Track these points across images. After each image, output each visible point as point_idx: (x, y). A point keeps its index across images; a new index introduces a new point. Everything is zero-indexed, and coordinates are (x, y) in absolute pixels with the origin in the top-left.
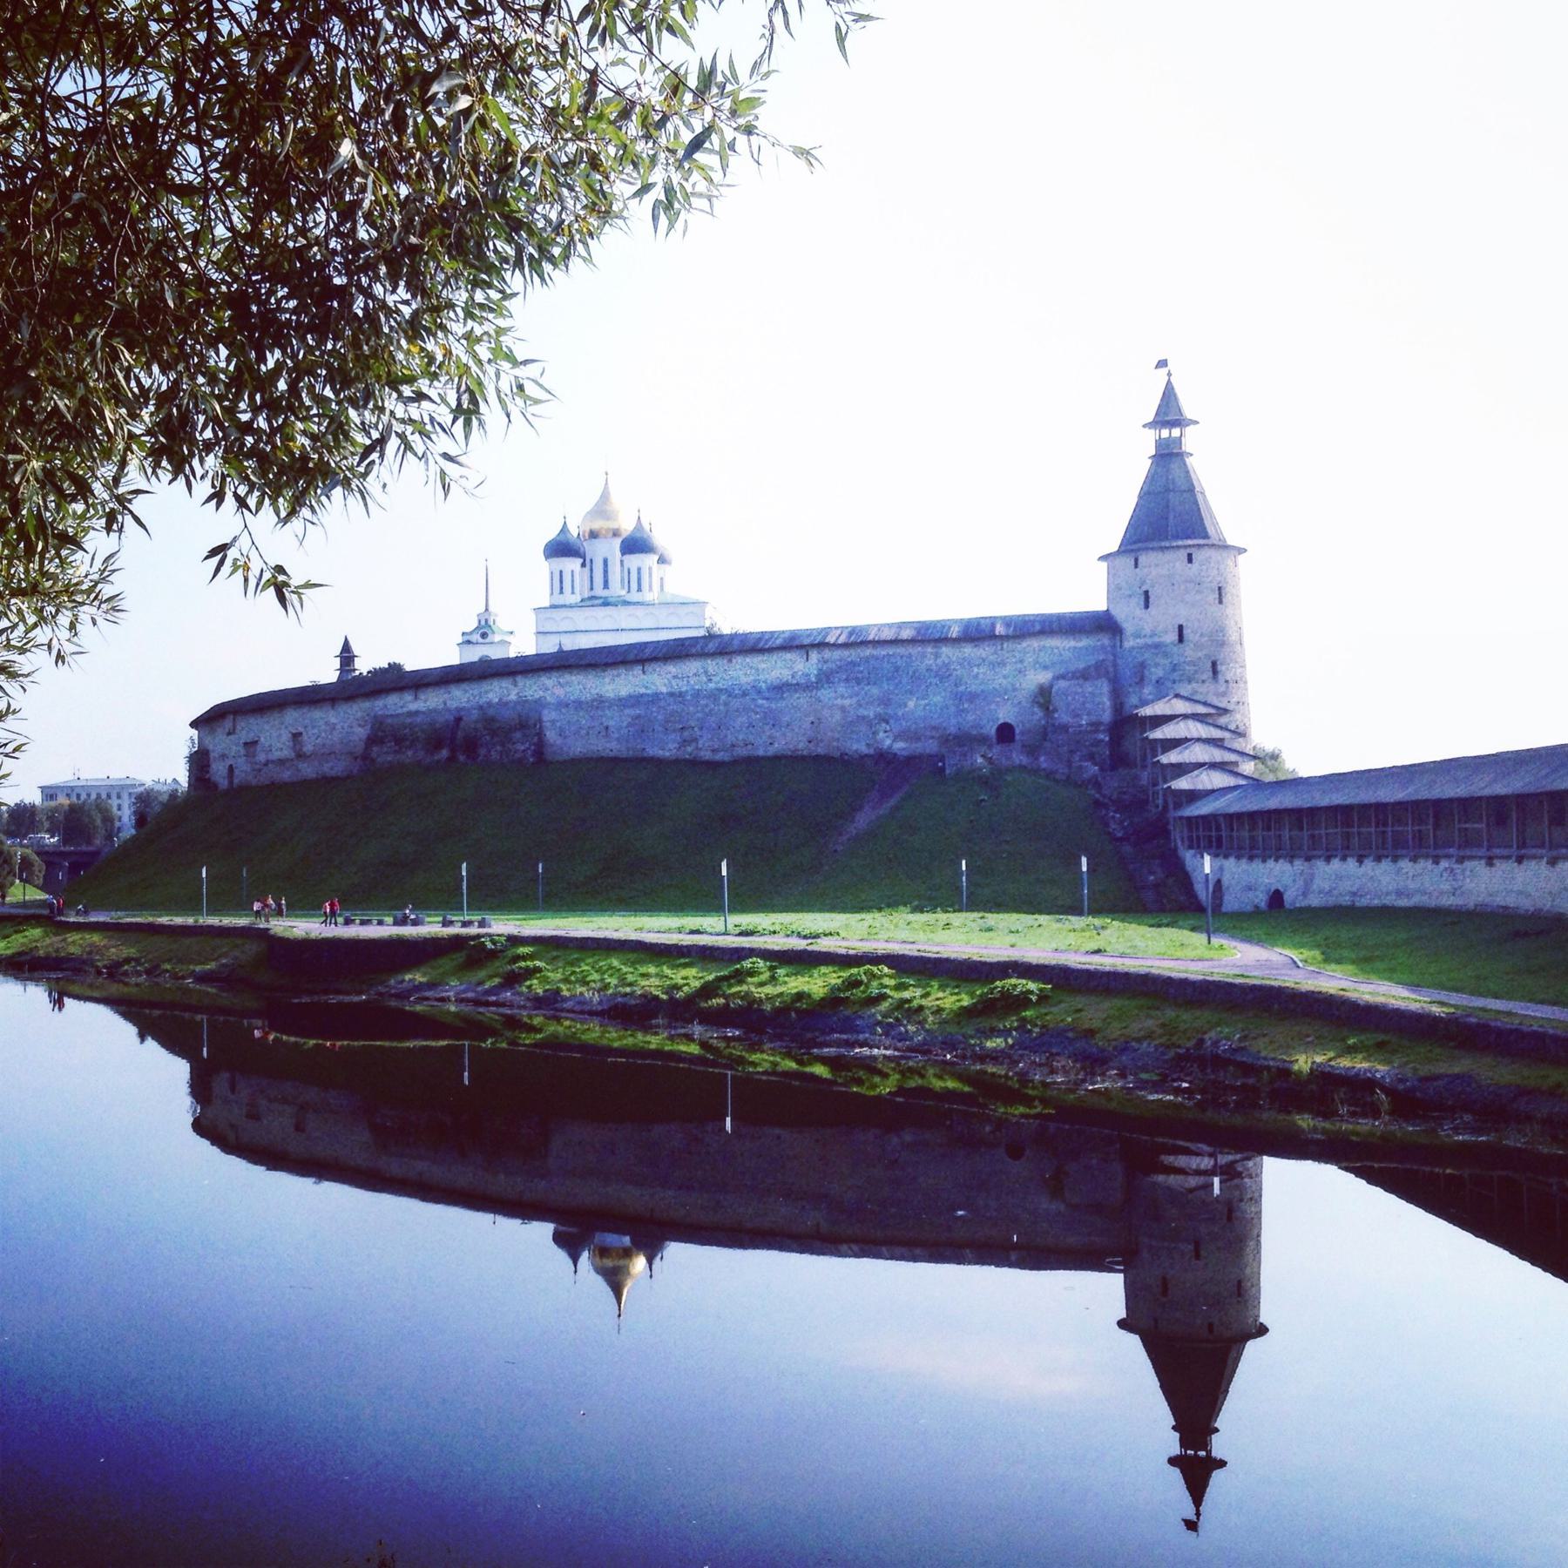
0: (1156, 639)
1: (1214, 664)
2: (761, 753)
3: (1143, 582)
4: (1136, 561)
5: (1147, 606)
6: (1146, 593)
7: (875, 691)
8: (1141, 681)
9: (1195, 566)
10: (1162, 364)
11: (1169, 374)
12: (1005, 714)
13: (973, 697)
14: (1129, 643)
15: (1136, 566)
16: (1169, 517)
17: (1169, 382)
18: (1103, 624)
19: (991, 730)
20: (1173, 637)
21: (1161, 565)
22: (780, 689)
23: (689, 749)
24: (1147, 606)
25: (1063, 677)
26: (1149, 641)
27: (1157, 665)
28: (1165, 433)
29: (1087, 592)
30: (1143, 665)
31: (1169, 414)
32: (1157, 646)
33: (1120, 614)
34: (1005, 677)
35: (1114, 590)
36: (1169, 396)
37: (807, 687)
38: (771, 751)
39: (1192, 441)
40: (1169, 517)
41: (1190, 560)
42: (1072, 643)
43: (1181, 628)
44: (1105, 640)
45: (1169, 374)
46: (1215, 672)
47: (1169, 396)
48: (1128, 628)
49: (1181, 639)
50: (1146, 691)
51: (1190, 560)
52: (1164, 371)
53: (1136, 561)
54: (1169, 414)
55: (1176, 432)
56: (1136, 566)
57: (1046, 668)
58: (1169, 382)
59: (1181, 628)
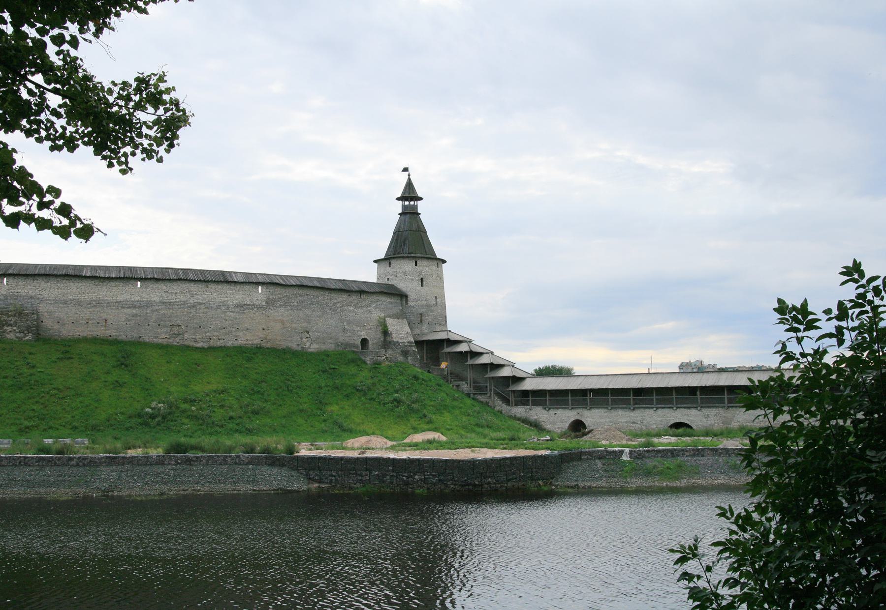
2: (229, 344)
3: (421, 274)
6: (422, 279)
7: (301, 313)
10: (406, 170)
12: (364, 335)
13: (349, 323)
17: (409, 180)
20: (433, 302)
22: (242, 307)
23: (177, 339)
25: (390, 317)
28: (407, 203)
31: (409, 195)
33: (403, 286)
36: (409, 185)
37: (260, 307)
38: (236, 344)
47: (409, 185)
48: (412, 295)
50: (424, 328)
54: (409, 195)
55: (412, 203)
58: (409, 180)
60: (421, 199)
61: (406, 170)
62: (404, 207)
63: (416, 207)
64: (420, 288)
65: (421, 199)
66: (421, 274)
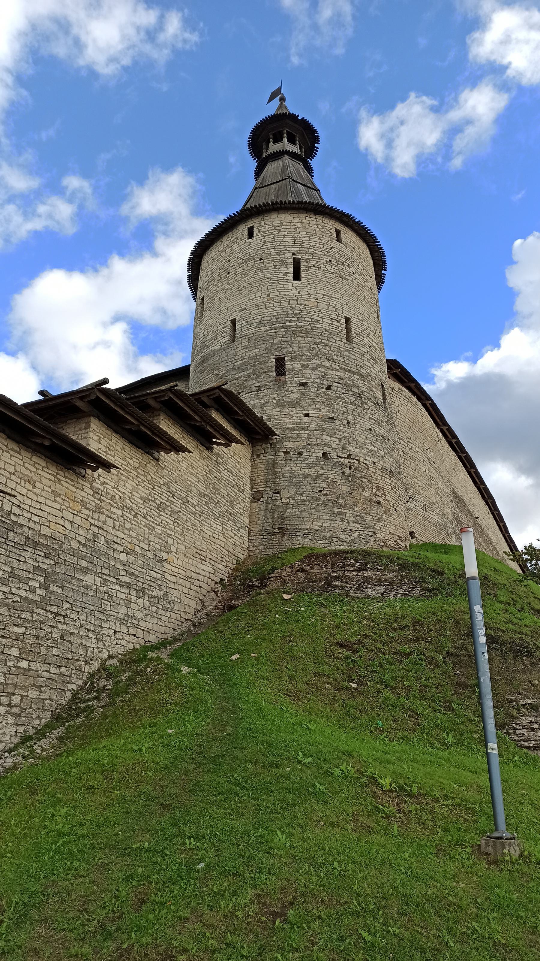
51: (251, 235)
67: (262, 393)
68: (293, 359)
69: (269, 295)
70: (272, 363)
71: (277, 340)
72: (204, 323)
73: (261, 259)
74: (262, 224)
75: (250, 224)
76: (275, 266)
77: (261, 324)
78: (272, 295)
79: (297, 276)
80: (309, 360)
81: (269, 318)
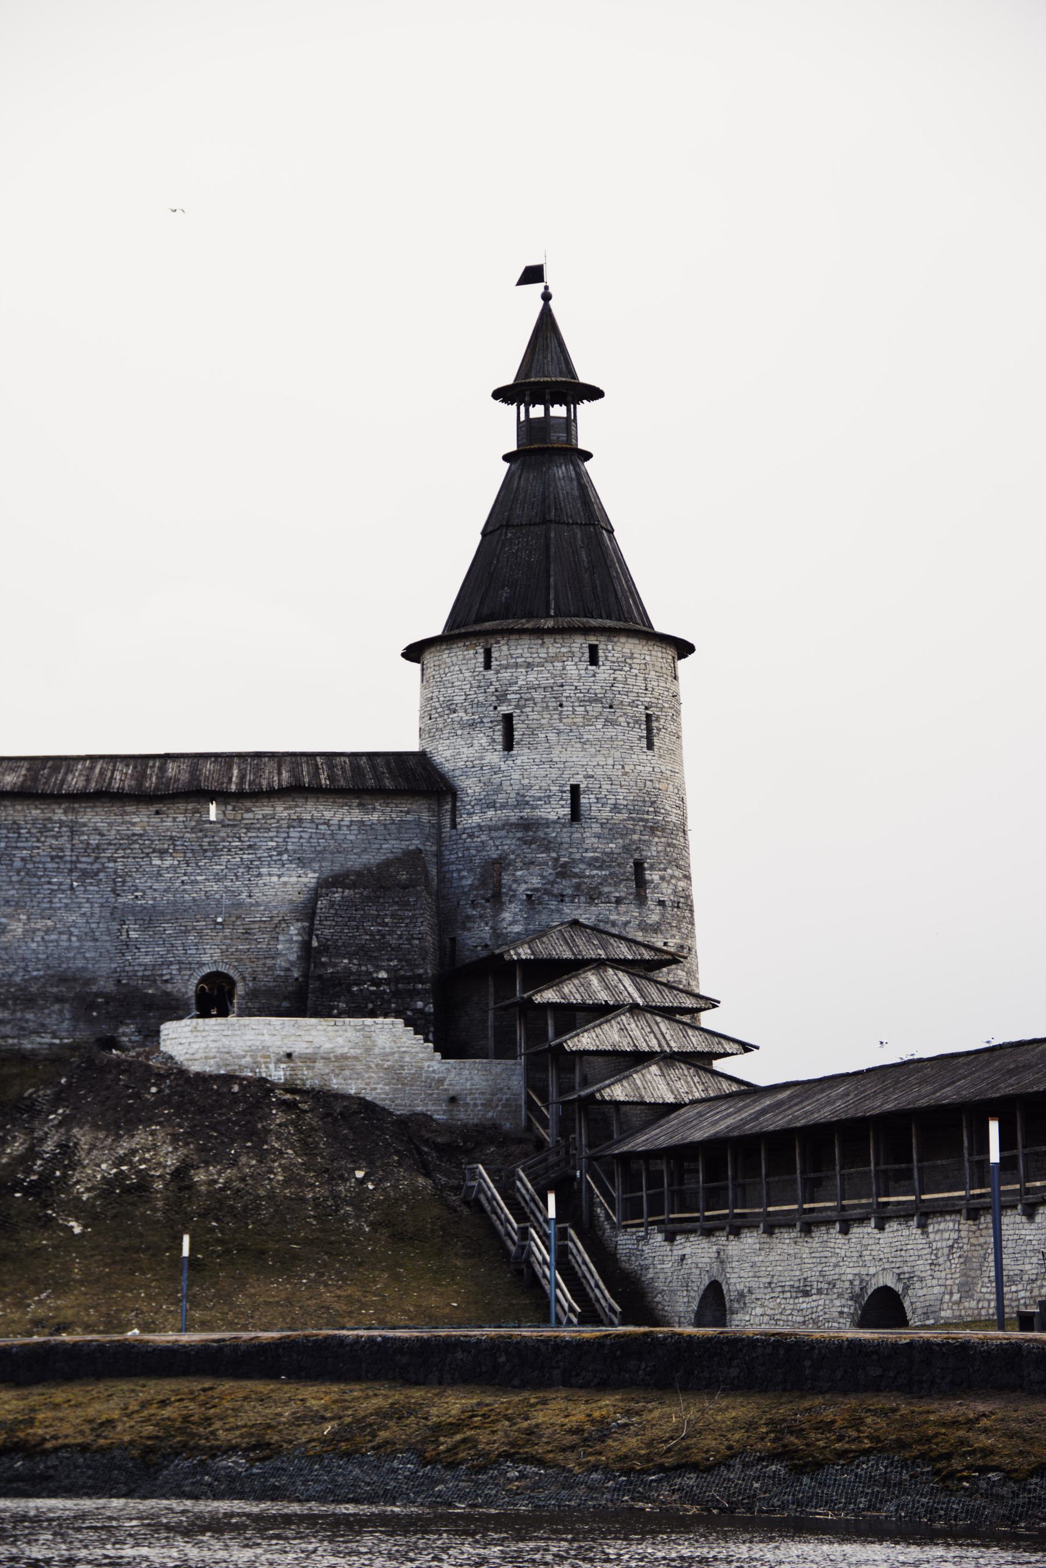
0: (526, 813)
1: (639, 867)
3: (502, 697)
4: (488, 654)
5: (509, 744)
6: (508, 720)
8: (497, 899)
9: (603, 672)
10: (533, 275)
11: (546, 297)
13: (149, 918)
14: (469, 820)
15: (487, 666)
16: (547, 568)
18: (408, 778)
19: (189, 987)
21: (540, 665)
24: (509, 744)
26: (513, 816)
27: (528, 864)
28: (537, 411)
29: (383, 714)
30: (500, 864)
31: (546, 378)
32: (527, 825)
33: (452, 754)
34: (219, 878)
35: (436, 713)
36: (546, 331)
39: (591, 425)
40: (547, 568)
41: (594, 660)
42: (356, 815)
43: (575, 790)
44: (418, 812)
45: (546, 297)
46: (641, 883)
47: (546, 331)
48: (470, 787)
49: (576, 814)
50: (507, 915)
51: (594, 660)
52: (538, 288)
53: (488, 654)
54: (546, 378)
55: (558, 411)
56: (487, 666)
57: (302, 862)
59: (575, 790)
60: (594, 393)
61: (533, 275)
62: (527, 429)
63: (569, 424)
64: (494, 757)
65: (594, 393)
66: (502, 697)
67: (622, 908)
68: (652, 868)
69: (623, 768)
70: (630, 868)
71: (635, 837)
72: (519, 762)
73: (611, 707)
74: (610, 647)
75: (593, 640)
76: (628, 723)
77: (615, 808)
78: (627, 769)
79: (650, 746)
80: (665, 869)
81: (625, 803)
